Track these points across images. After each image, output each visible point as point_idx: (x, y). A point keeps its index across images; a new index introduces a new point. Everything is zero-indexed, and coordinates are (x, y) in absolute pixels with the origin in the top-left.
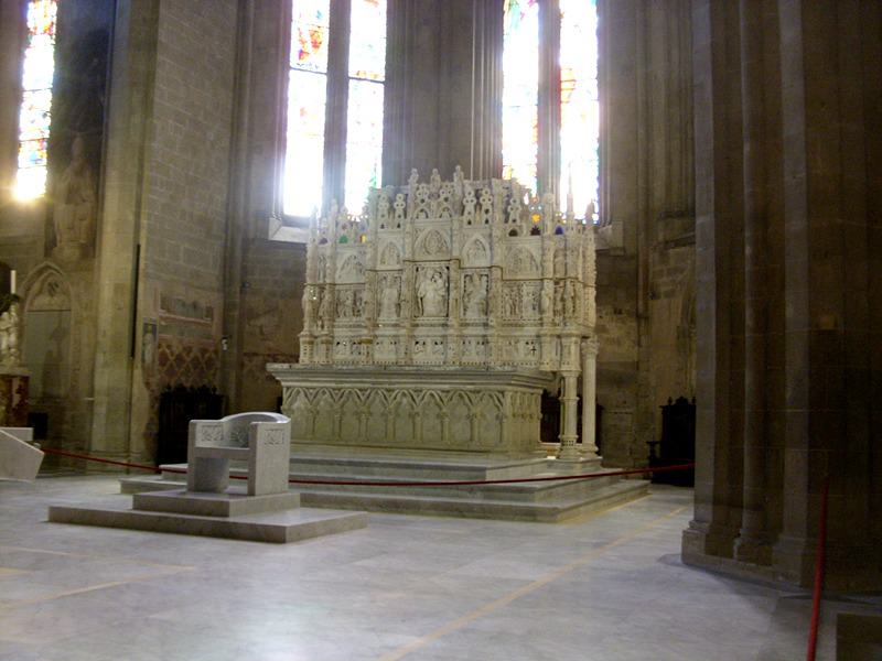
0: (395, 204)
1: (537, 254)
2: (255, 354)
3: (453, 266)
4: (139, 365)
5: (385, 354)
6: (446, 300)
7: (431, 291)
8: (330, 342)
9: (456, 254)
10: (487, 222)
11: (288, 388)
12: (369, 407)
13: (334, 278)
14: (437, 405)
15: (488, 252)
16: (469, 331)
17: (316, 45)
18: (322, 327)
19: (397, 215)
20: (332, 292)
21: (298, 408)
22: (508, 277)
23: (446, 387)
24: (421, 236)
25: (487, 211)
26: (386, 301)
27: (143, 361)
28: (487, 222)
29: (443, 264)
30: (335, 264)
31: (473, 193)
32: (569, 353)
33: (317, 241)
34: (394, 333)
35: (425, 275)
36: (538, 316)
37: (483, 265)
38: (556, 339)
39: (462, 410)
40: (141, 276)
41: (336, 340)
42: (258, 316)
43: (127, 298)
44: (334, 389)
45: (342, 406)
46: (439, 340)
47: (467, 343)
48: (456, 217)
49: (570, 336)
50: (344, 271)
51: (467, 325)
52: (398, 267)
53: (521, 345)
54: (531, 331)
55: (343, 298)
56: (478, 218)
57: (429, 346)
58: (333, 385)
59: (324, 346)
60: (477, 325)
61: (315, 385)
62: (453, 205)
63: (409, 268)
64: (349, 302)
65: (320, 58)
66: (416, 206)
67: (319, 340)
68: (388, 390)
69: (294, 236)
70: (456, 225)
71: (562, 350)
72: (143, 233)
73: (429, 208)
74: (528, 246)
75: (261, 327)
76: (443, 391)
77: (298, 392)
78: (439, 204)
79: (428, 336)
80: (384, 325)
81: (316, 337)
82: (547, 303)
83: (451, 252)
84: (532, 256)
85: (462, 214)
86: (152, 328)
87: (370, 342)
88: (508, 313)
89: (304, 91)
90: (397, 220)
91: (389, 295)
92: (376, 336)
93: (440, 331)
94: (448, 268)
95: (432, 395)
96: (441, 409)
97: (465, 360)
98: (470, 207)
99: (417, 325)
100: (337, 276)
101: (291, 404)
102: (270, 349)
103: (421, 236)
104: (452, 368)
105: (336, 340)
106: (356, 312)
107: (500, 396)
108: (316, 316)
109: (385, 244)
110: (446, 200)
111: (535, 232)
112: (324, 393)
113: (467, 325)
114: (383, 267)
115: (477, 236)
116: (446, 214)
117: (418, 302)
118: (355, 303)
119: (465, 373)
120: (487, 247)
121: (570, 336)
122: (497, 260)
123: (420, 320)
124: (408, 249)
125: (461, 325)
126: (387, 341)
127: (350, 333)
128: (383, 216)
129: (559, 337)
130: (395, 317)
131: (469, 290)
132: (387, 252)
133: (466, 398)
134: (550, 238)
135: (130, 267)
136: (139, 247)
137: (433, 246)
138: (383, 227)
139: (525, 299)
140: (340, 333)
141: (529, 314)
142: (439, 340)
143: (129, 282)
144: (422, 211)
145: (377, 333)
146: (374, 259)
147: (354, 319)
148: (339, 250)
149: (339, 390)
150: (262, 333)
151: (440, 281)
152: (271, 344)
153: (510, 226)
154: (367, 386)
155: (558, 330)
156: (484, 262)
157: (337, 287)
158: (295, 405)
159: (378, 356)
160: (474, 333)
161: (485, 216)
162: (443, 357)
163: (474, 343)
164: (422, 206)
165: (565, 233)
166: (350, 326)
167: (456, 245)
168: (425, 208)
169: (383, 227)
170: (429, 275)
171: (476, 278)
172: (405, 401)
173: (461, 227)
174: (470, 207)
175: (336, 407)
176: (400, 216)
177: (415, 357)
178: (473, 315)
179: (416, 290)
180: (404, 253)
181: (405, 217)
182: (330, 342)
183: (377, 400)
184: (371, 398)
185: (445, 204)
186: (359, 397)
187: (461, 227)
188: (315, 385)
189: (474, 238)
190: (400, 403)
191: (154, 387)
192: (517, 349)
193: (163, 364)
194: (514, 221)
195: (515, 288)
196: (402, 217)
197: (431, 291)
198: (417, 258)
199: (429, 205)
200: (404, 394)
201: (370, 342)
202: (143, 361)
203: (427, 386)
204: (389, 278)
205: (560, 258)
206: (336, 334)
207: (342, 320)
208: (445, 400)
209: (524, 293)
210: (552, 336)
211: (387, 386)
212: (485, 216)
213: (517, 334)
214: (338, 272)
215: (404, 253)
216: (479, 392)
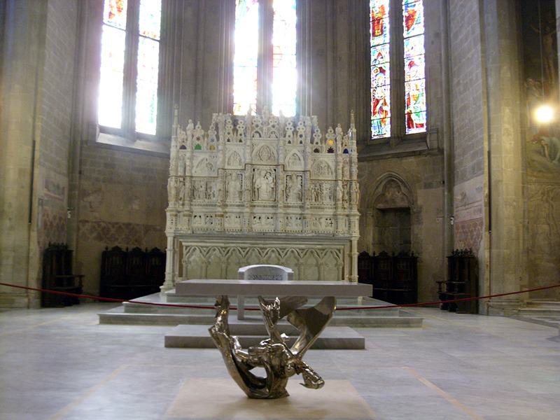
0: (238, 126)
1: (332, 165)
2: (87, 222)
3: (280, 169)
4: (36, 229)
5: (232, 224)
6: (275, 190)
7: (264, 184)
8: (190, 215)
9: (281, 161)
10: (301, 143)
11: (187, 247)
12: (247, 259)
13: (191, 173)
14: (295, 257)
15: (302, 162)
16: (290, 211)
17: (119, 10)
18: (183, 205)
19: (239, 134)
20: (191, 182)
21: (194, 260)
22: (314, 178)
23: (303, 246)
24: (256, 149)
25: (301, 136)
26: (231, 190)
27: (38, 225)
28: (301, 143)
29: (272, 168)
30: (192, 163)
31: (292, 124)
32: (355, 226)
33: (178, 148)
34: (239, 210)
35: (260, 174)
36: (333, 203)
37: (299, 170)
38: (347, 218)
39: (312, 261)
40: (35, 164)
41: (194, 214)
42: (89, 194)
43: (28, 180)
44: (222, 248)
45: (228, 259)
46: (270, 216)
47: (289, 218)
48: (282, 138)
49: (355, 215)
50: (198, 168)
51: (289, 207)
52: (240, 168)
53: (323, 220)
54: (330, 212)
55: (197, 186)
56: (295, 139)
57: (263, 220)
58: (222, 245)
59: (186, 218)
60: (296, 207)
61: (208, 245)
62: (279, 130)
63: (249, 167)
64: (203, 189)
65: (121, 19)
66: (253, 129)
67: (182, 214)
68: (261, 249)
69: (109, 140)
70: (281, 143)
71: (349, 224)
72: (38, 133)
73: (262, 131)
74: (326, 159)
75: (90, 203)
76: (300, 249)
77: (195, 250)
78: (269, 129)
79: (263, 213)
80: (231, 206)
81: (179, 212)
82: (340, 195)
83: (278, 160)
84: (329, 166)
85: (285, 136)
86: (41, 202)
87: (222, 216)
88: (314, 201)
89: (111, 39)
90: (239, 137)
91: (234, 186)
92: (226, 212)
93: (271, 210)
94: (275, 170)
95: (292, 252)
96: (298, 260)
97: (288, 228)
98: (289, 132)
99: (254, 206)
100: (193, 172)
101: (189, 258)
102: (96, 218)
103: (256, 149)
104: (310, 235)
105: (194, 214)
106: (207, 196)
107: (337, 252)
108: (178, 198)
109: (230, 153)
110: (273, 126)
111: (330, 151)
112: (214, 250)
113: (289, 207)
114: (229, 167)
115: (295, 151)
116: (273, 135)
117: (254, 191)
118: (206, 190)
119: (319, 238)
120: (302, 158)
121: (355, 215)
122: (309, 167)
123: (256, 203)
124: (248, 156)
125: (285, 207)
126: (233, 216)
127: (204, 210)
128: (229, 133)
129: (347, 216)
130: (238, 200)
131: (290, 185)
132: (232, 158)
133: (316, 254)
134: (341, 155)
135: (29, 156)
136: (34, 142)
137: (265, 156)
138: (229, 141)
139: (325, 192)
140: (197, 210)
141: (327, 202)
142: (270, 216)
143: (28, 168)
144: (257, 132)
145: (227, 210)
146: (224, 161)
147: (207, 200)
148: (194, 154)
149: (226, 248)
150: (91, 207)
151: (271, 179)
152: (97, 215)
153: (315, 146)
154: (246, 245)
155: (347, 212)
156: (300, 168)
157: (194, 179)
158: (191, 259)
159: (227, 225)
160: (295, 212)
161: (300, 139)
162: (273, 227)
163: (294, 219)
164: (257, 129)
165: (350, 152)
166: (204, 205)
167: (281, 156)
168: (259, 130)
169: (229, 141)
170: (263, 173)
171: (294, 177)
172: (273, 255)
173: (285, 145)
174: (289, 132)
175: (224, 259)
176: (241, 135)
177: (253, 226)
178: (292, 200)
179: (253, 183)
180: (245, 159)
181: (245, 136)
182: (190, 215)
183: (254, 255)
184: (249, 253)
185: (273, 129)
186: (240, 253)
187: (285, 145)
188: (208, 245)
189: (291, 153)
190: (270, 257)
191: (41, 245)
192: (320, 223)
193: (45, 229)
194: (317, 143)
195: (318, 185)
196: (243, 136)
197: (264, 184)
198: (254, 163)
199: (262, 129)
200: (273, 251)
201: (222, 216)
202: (38, 225)
203: (291, 246)
204: (234, 175)
205: (347, 168)
206: (194, 210)
207: (197, 201)
208: (302, 255)
209: (324, 188)
210: (343, 215)
211: (262, 246)
212: (300, 139)
213: (322, 213)
214: (194, 168)
215: (245, 159)
216: (324, 250)
